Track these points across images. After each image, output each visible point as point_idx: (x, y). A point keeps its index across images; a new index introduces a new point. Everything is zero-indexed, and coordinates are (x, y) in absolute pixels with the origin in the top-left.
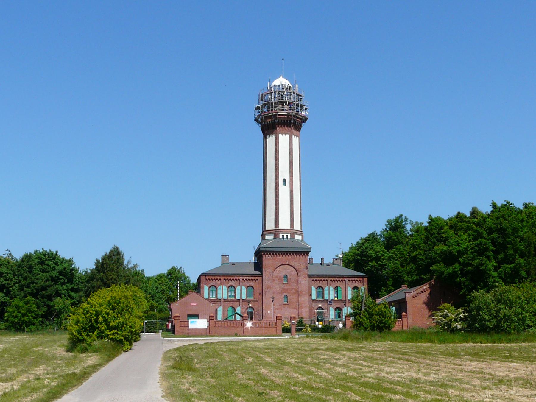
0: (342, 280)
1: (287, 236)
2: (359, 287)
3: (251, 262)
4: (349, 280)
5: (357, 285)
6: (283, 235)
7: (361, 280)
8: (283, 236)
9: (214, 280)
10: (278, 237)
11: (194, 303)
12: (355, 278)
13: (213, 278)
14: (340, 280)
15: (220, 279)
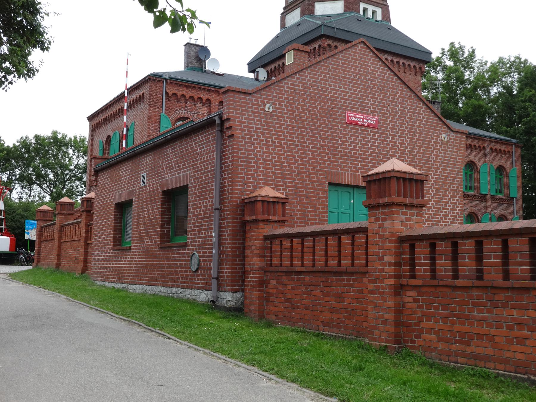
0: (479, 146)
1: (374, 12)
2: (507, 167)
3: (259, 79)
4: (491, 149)
5: (503, 163)
6: (367, 9)
7: (511, 151)
8: (365, 10)
9: (190, 103)
10: (355, 11)
11: (363, 112)
12: (501, 145)
13: (188, 93)
14: (477, 145)
15: (209, 100)
